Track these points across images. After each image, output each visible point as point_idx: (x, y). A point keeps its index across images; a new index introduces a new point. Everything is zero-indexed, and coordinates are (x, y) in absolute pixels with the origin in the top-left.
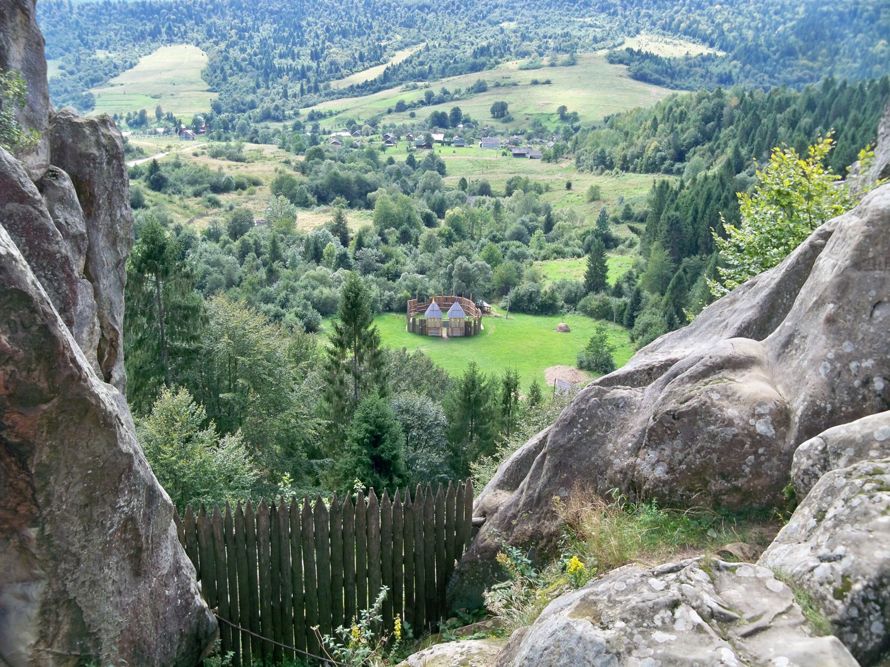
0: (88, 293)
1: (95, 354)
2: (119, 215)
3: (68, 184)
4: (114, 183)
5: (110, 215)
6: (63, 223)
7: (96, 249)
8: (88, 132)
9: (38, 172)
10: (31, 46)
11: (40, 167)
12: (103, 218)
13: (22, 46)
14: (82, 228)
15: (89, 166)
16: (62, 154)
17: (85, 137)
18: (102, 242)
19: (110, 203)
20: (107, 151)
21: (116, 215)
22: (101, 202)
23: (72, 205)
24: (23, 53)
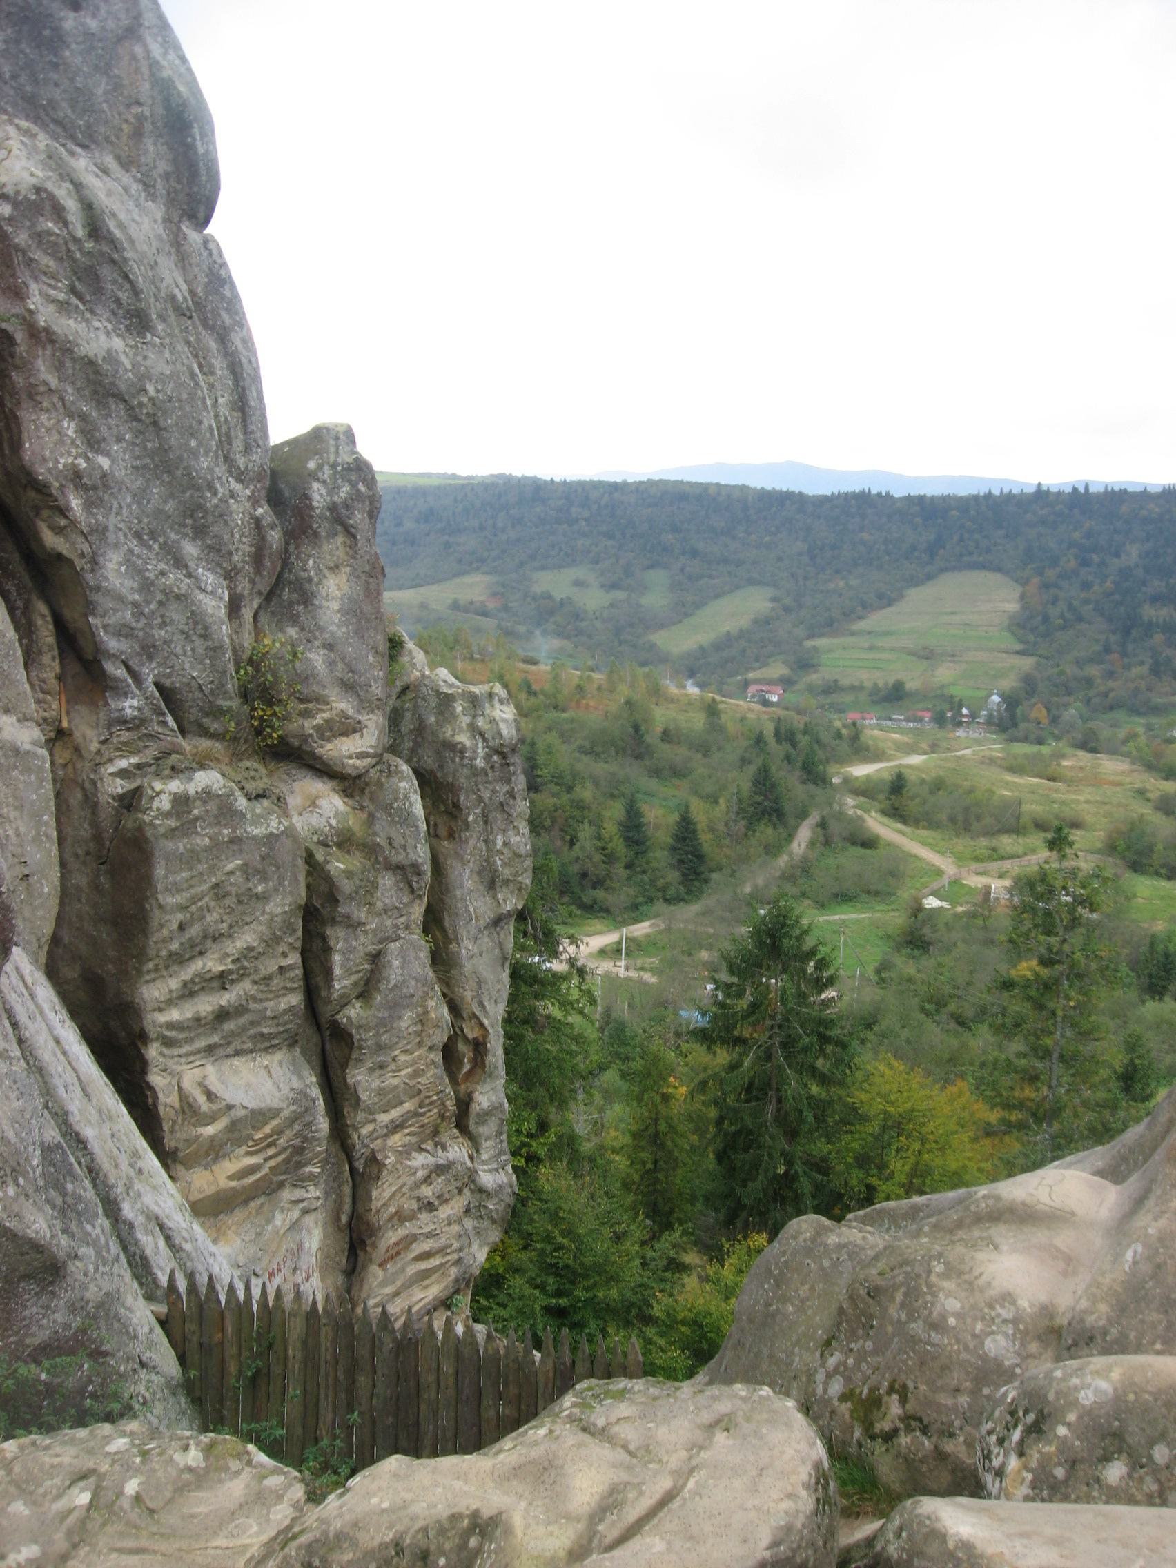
0: (418, 958)
1: (437, 1057)
2: (500, 842)
3: (406, 786)
4: (494, 791)
5: (486, 841)
6: (384, 843)
7: (458, 893)
8: (459, 709)
9: (358, 762)
10: (358, 577)
11: (362, 755)
12: (473, 842)
13: (345, 578)
14: (422, 854)
15: (453, 761)
16: (419, 739)
17: (454, 716)
18: (465, 879)
19: (486, 822)
20: (485, 740)
21: (495, 843)
22: (471, 818)
23: (406, 819)
24: (346, 588)
